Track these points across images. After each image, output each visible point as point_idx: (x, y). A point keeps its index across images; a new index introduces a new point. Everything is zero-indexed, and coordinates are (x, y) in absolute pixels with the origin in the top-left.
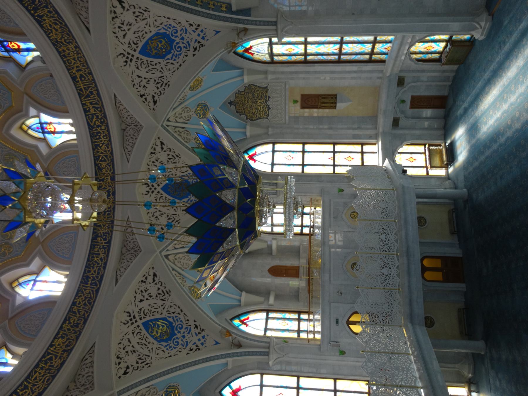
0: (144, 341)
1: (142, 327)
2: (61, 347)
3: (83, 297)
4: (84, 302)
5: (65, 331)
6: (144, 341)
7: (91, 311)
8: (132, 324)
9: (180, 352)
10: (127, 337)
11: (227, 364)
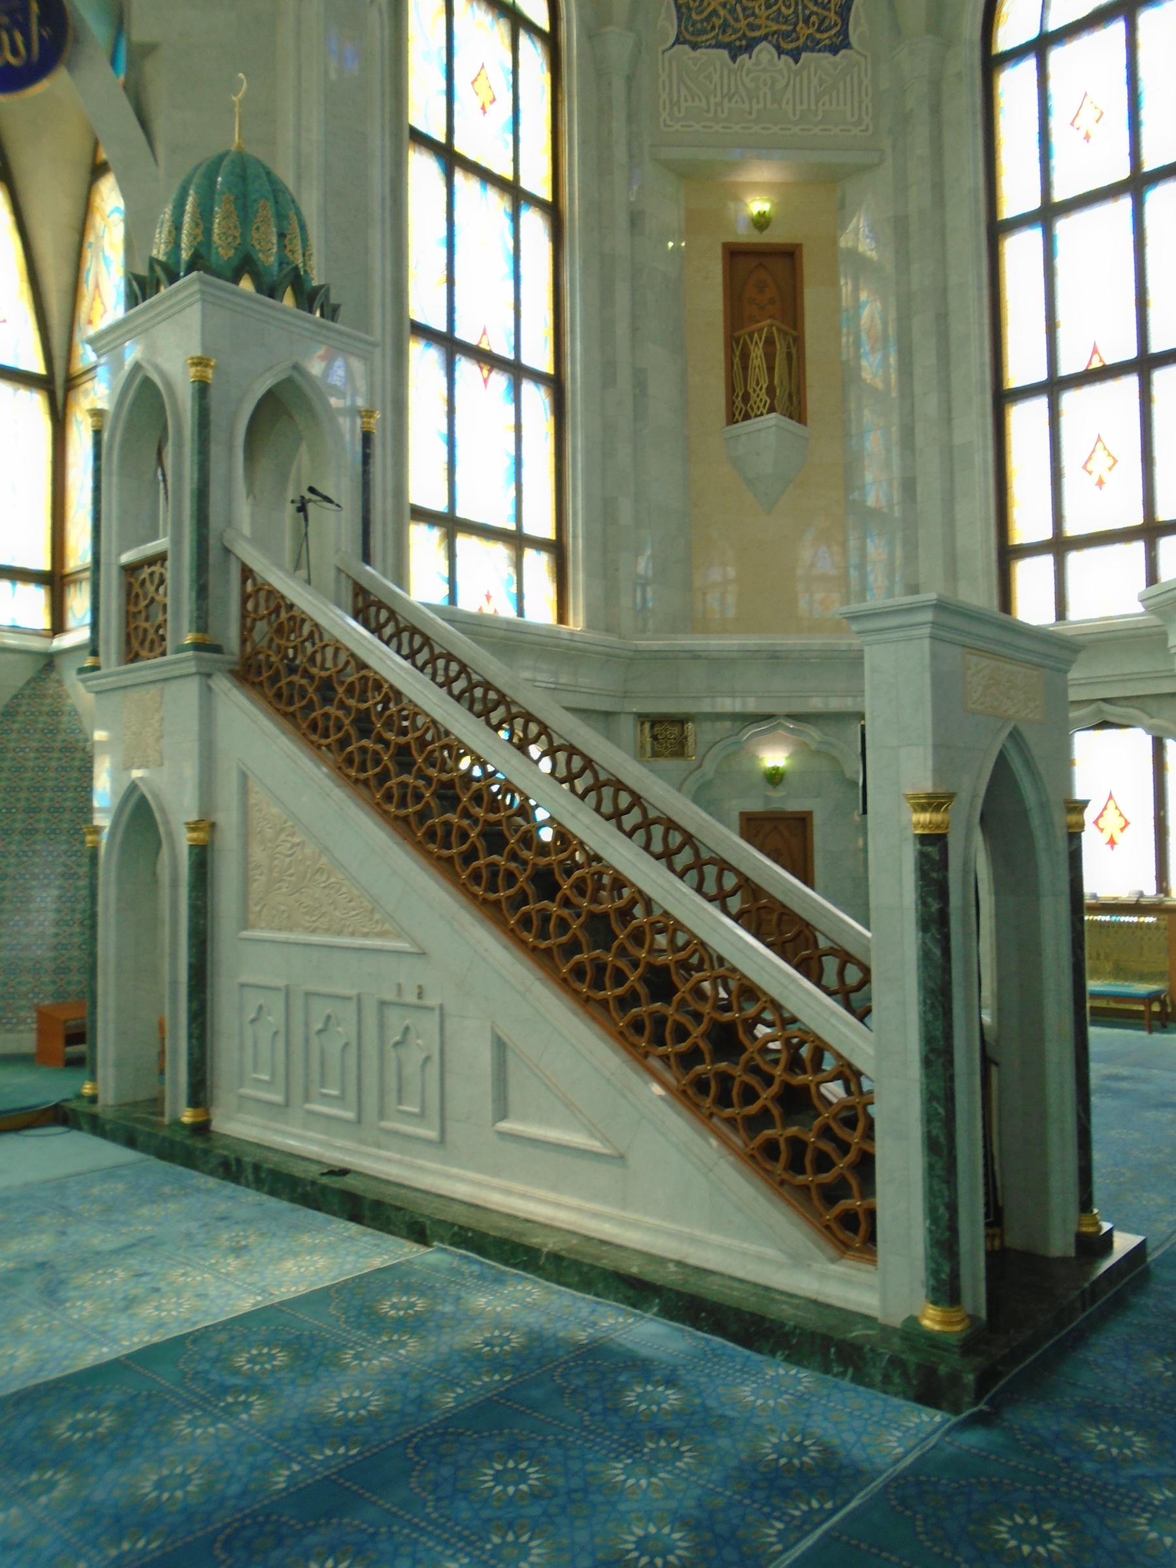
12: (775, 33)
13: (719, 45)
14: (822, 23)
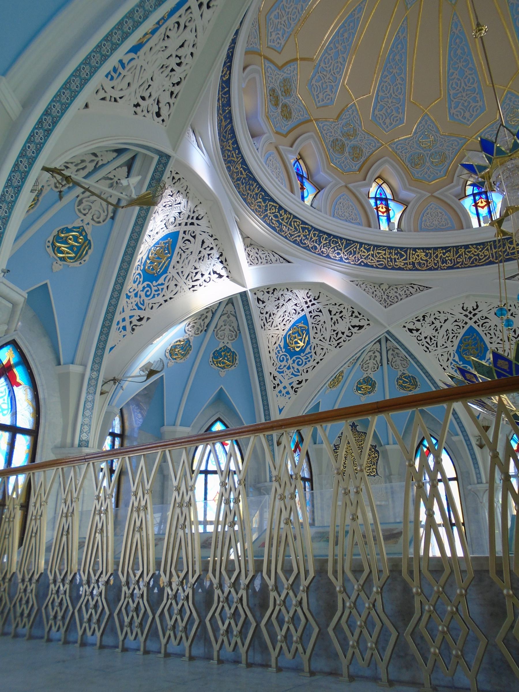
0: (451, 336)
1: (467, 327)
2: (416, 259)
3: (478, 252)
4: (472, 255)
5: (434, 254)
6: (451, 336)
7: (465, 267)
8: (466, 316)
10: (449, 316)
11: (457, 435)
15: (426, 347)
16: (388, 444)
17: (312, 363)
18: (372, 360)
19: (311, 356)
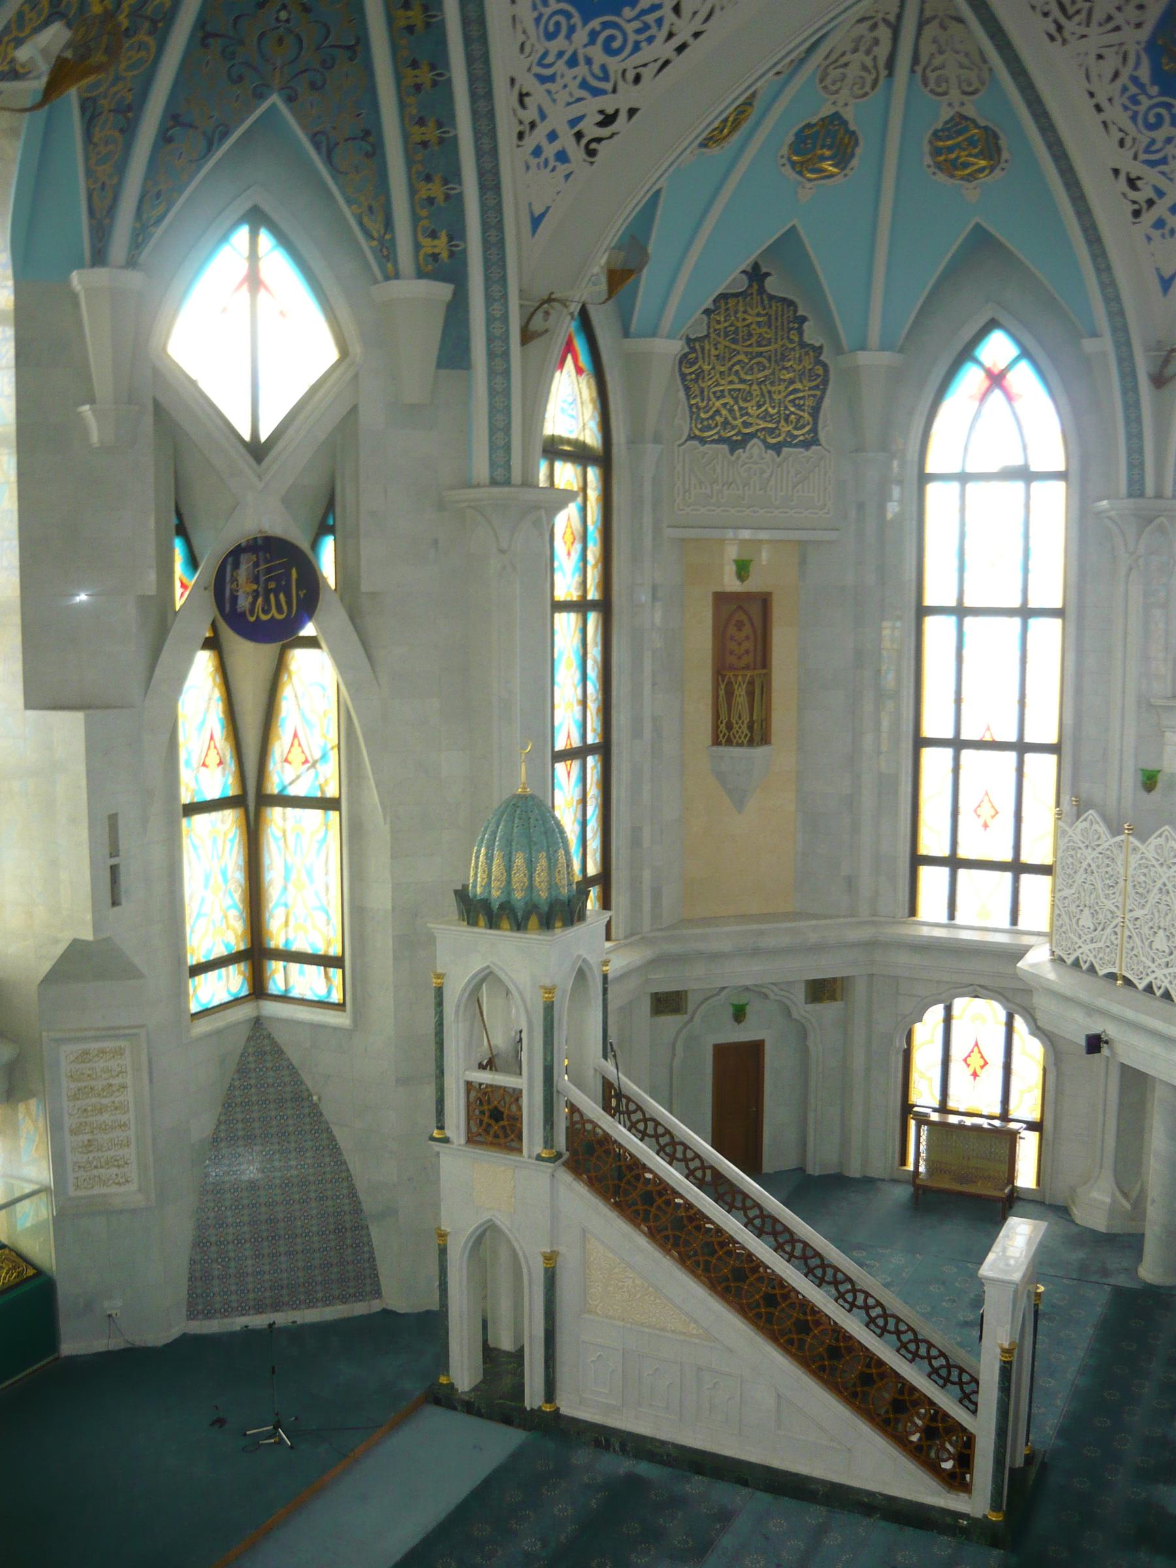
9: (1122, 143)
12: (763, 429)
13: (721, 440)
14: (798, 421)
15: (1056, 22)
16: (863, 348)
17: (661, 49)
18: (860, 56)
19: (660, 22)
